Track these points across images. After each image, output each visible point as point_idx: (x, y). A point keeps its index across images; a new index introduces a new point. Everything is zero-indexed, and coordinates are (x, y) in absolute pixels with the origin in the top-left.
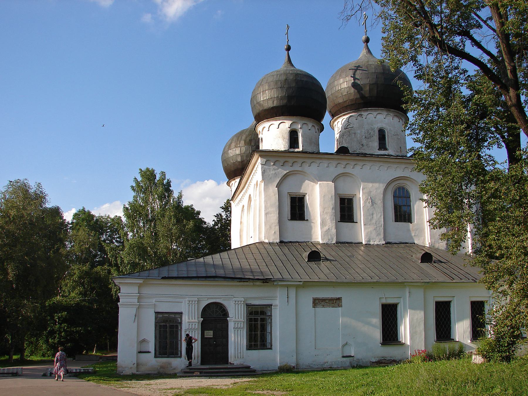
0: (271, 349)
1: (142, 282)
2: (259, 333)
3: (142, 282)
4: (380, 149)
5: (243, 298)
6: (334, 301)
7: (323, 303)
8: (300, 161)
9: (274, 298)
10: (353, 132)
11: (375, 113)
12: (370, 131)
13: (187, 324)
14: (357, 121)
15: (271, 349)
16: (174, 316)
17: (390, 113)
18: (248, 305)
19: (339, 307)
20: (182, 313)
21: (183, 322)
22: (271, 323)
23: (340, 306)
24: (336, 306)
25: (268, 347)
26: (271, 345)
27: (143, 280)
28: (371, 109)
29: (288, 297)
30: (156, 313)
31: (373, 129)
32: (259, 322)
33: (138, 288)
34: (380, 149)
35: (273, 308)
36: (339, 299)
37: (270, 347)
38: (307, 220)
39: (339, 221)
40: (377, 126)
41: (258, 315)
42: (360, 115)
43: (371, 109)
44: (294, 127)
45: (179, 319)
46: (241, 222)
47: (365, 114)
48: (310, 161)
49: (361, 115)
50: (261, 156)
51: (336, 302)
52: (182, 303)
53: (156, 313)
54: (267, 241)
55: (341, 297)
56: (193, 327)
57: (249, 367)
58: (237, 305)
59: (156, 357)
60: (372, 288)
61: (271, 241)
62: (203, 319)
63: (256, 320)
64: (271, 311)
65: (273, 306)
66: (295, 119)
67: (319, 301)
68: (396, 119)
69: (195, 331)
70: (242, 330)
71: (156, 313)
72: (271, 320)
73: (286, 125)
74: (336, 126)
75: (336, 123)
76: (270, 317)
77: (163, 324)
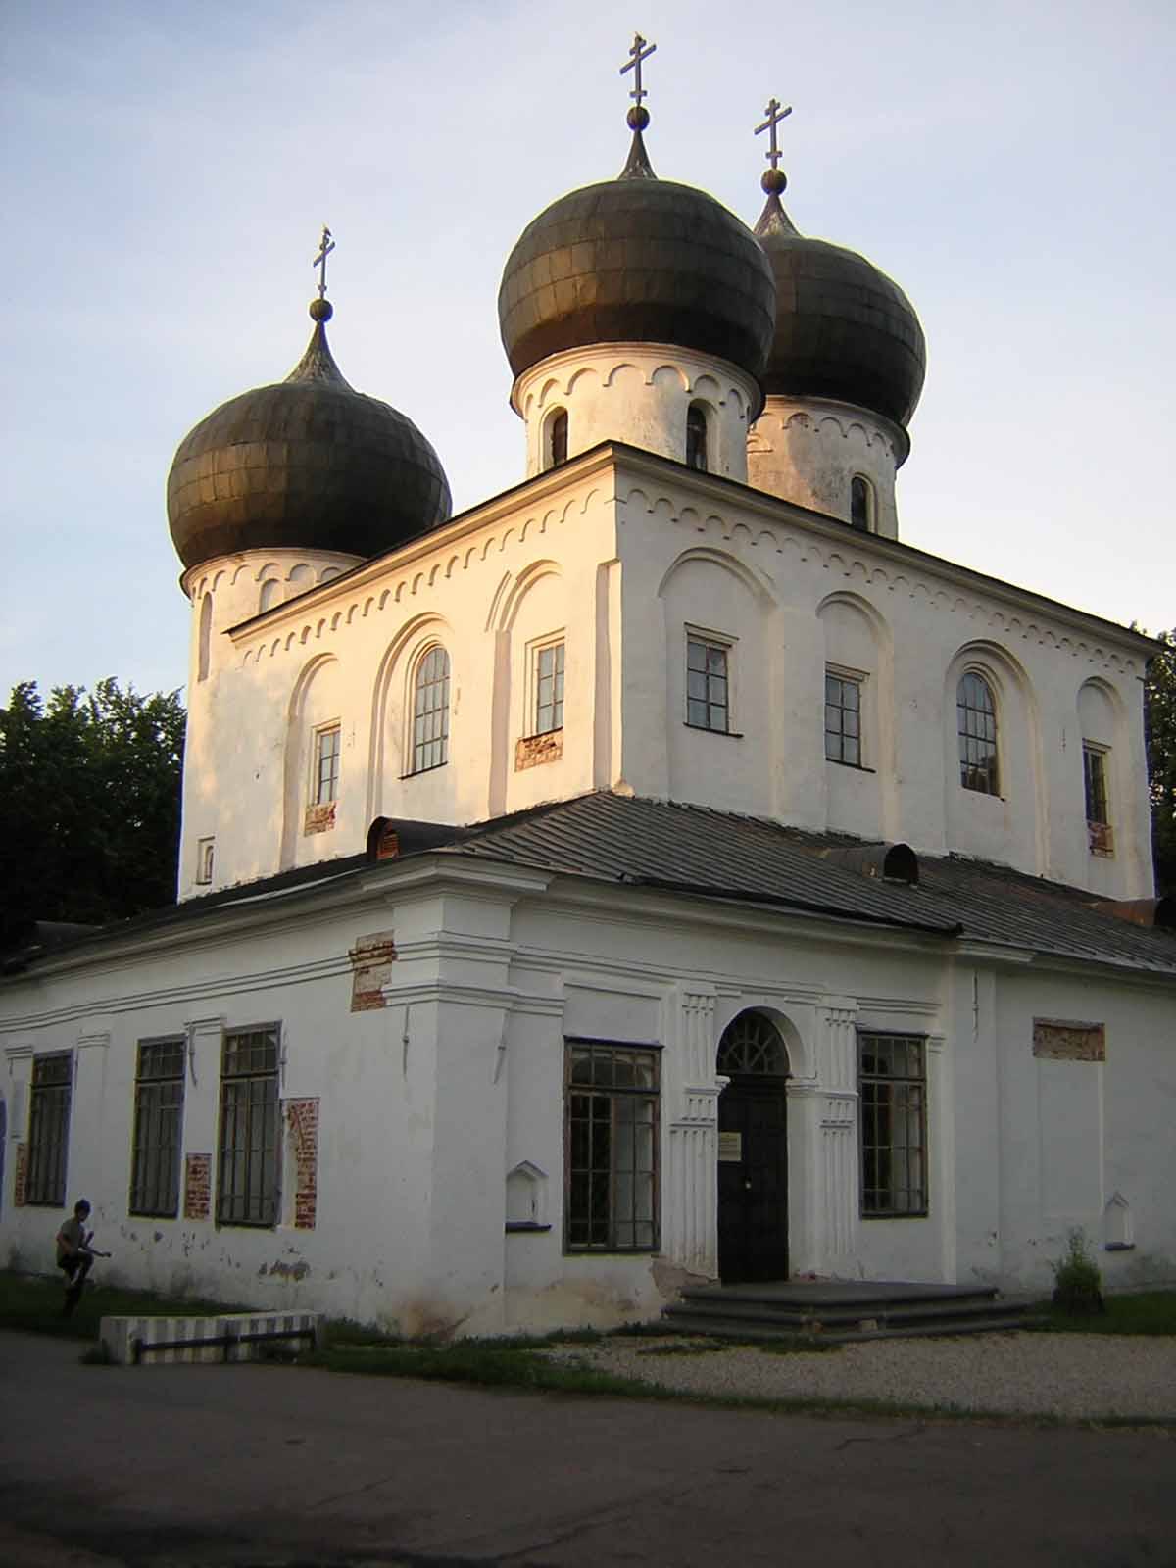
0: (924, 1214)
1: (543, 887)
3: (543, 887)
5: (854, 1000)
6: (1084, 1039)
8: (731, 518)
9: (929, 1008)
11: (847, 422)
13: (683, 1100)
15: (924, 1214)
16: (627, 1059)
17: (883, 434)
18: (859, 1032)
19: (1094, 1060)
20: (660, 1048)
21: (665, 1090)
22: (921, 1109)
23: (1101, 1057)
24: (1086, 1056)
25: (902, 1207)
26: (925, 1202)
27: (548, 879)
28: (838, 406)
29: (976, 1010)
30: (571, 1041)
31: (838, 471)
33: (509, 910)
35: (928, 1046)
36: (1097, 1030)
37: (918, 1207)
38: (739, 736)
40: (847, 467)
41: (872, 1070)
42: (799, 418)
43: (838, 406)
44: (706, 393)
45: (648, 1077)
47: (817, 416)
48: (756, 526)
50: (621, 468)
51: (1083, 1041)
52: (659, 1002)
53: (569, 1040)
54: (629, 792)
55: (1103, 1025)
57: (989, 1294)
59: (569, 1251)
61: (643, 795)
62: (727, 1079)
64: (921, 1062)
65: (928, 1041)
66: (709, 366)
67: (1045, 1032)
69: (704, 1133)
71: (571, 1041)
72: (923, 1097)
73: (685, 380)
76: (917, 1084)
77: (596, 1094)
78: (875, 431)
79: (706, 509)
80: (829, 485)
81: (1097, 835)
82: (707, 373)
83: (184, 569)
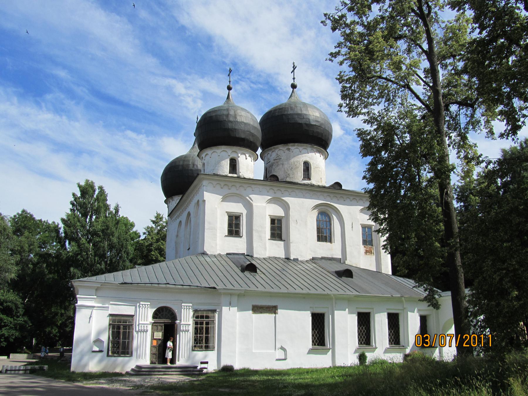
2: (204, 335)
4: (304, 178)
6: (271, 309)
7: (260, 310)
8: (238, 185)
10: (281, 163)
11: (301, 148)
12: (296, 163)
14: (285, 154)
28: (297, 145)
30: (111, 315)
32: (204, 326)
33: (95, 291)
34: (304, 178)
39: (270, 238)
44: (233, 155)
46: (177, 236)
49: (289, 149)
56: (140, 329)
58: (185, 309)
60: (304, 298)
63: (202, 323)
68: (318, 155)
70: (186, 333)
74: (266, 158)
75: (266, 155)
78: (310, 149)
79: (230, 184)
80: (296, 165)
81: (368, 249)
82: (234, 150)
83: (262, 179)
